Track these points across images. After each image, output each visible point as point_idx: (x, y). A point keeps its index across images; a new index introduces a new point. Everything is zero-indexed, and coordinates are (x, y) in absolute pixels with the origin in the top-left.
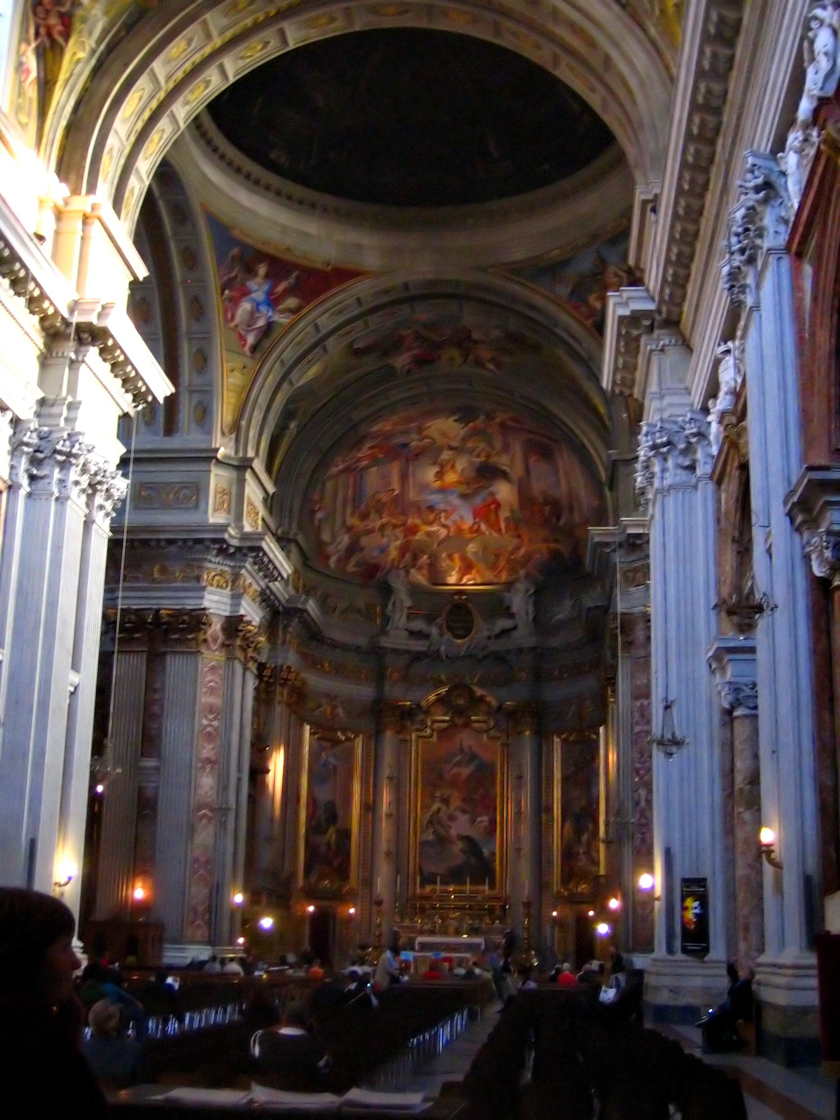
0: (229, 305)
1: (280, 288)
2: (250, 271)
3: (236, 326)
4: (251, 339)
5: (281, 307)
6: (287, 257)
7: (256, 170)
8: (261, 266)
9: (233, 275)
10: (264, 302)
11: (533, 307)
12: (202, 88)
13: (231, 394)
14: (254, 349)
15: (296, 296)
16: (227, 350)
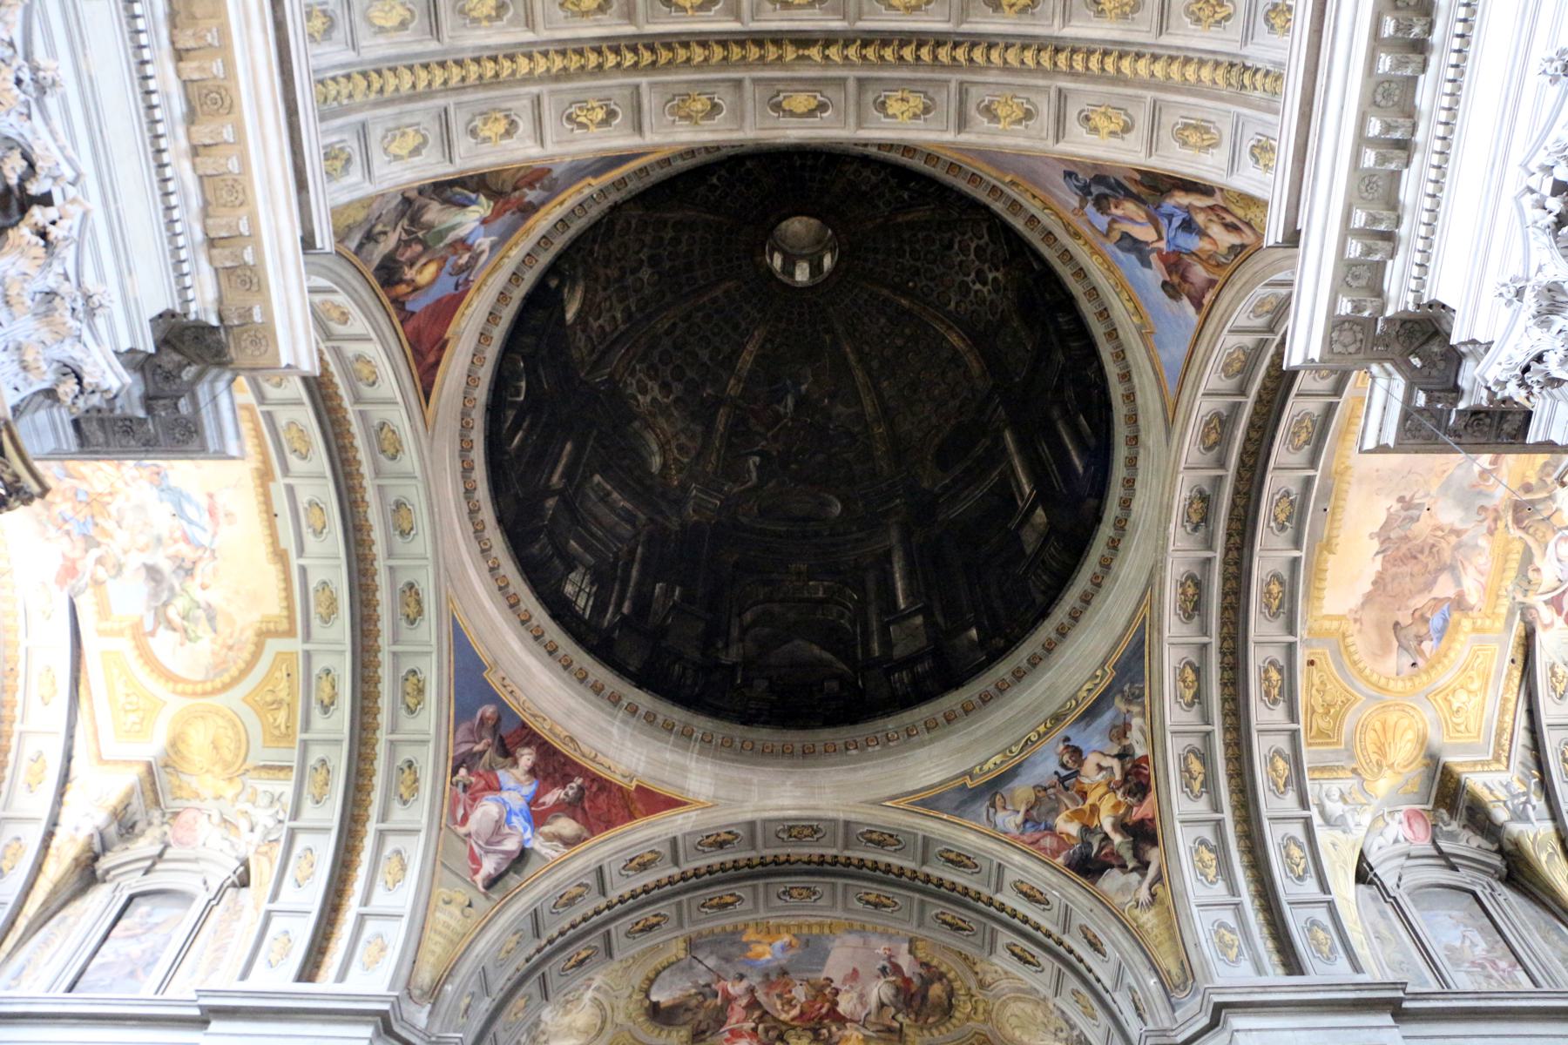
0: (462, 796)
1: (551, 798)
2: (506, 751)
3: (469, 835)
4: (489, 866)
5: (546, 829)
6: (566, 750)
7: (541, 616)
8: (526, 751)
9: (478, 748)
10: (521, 811)
11: (959, 861)
12: (501, 126)
13: (437, 938)
14: (492, 882)
15: (574, 818)
16: (443, 864)
